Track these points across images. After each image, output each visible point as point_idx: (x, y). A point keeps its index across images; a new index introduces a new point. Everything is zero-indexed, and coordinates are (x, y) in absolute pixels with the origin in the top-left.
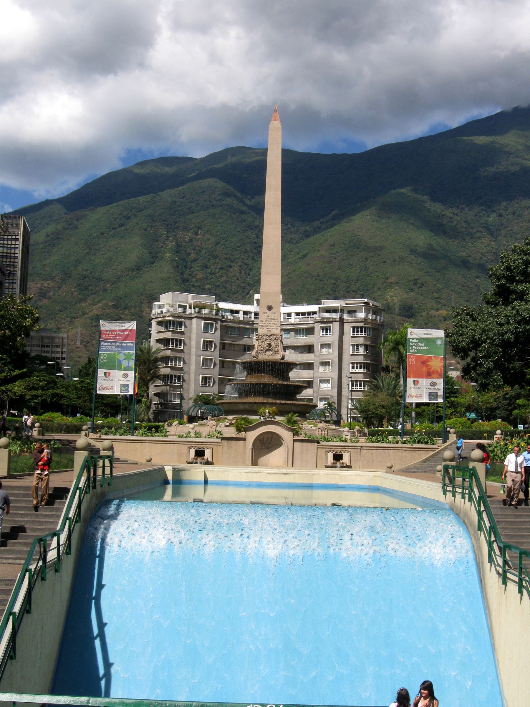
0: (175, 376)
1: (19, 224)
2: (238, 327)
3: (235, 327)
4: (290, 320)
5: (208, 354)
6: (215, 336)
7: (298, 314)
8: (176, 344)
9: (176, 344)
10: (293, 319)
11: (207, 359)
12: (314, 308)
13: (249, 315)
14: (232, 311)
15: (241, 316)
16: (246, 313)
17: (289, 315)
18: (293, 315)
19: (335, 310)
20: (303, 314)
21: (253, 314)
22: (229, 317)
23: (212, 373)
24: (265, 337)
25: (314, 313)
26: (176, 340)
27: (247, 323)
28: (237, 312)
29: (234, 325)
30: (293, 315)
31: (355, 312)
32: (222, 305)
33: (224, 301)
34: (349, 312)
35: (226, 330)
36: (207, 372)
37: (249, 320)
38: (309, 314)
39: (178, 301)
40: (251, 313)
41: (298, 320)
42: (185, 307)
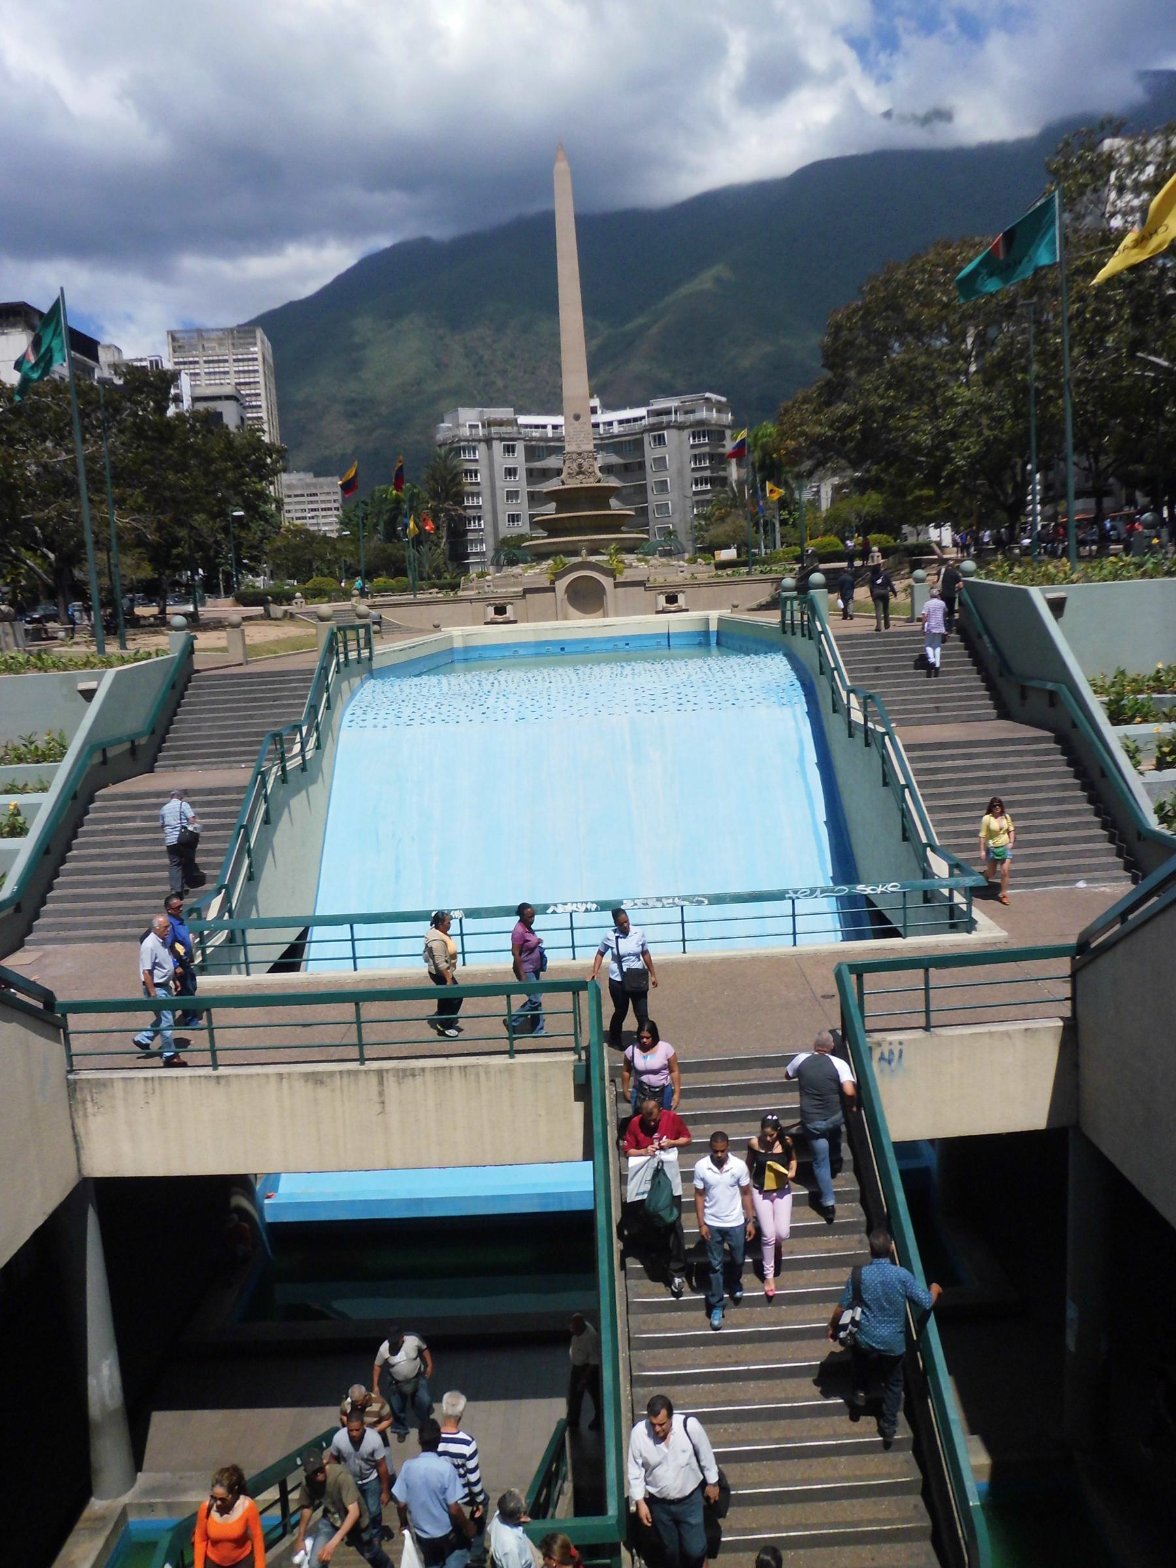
2: (547, 447)
5: (511, 484)
6: (518, 460)
7: (621, 422)
10: (616, 429)
12: (641, 412)
14: (537, 427)
16: (555, 427)
17: (610, 424)
18: (615, 424)
19: (667, 412)
20: (628, 421)
24: (574, 456)
26: (471, 471)
28: (544, 427)
29: (542, 444)
30: (615, 424)
31: (693, 412)
32: (523, 420)
33: (528, 412)
34: (687, 413)
35: (532, 453)
38: (635, 420)
42: (477, 426)
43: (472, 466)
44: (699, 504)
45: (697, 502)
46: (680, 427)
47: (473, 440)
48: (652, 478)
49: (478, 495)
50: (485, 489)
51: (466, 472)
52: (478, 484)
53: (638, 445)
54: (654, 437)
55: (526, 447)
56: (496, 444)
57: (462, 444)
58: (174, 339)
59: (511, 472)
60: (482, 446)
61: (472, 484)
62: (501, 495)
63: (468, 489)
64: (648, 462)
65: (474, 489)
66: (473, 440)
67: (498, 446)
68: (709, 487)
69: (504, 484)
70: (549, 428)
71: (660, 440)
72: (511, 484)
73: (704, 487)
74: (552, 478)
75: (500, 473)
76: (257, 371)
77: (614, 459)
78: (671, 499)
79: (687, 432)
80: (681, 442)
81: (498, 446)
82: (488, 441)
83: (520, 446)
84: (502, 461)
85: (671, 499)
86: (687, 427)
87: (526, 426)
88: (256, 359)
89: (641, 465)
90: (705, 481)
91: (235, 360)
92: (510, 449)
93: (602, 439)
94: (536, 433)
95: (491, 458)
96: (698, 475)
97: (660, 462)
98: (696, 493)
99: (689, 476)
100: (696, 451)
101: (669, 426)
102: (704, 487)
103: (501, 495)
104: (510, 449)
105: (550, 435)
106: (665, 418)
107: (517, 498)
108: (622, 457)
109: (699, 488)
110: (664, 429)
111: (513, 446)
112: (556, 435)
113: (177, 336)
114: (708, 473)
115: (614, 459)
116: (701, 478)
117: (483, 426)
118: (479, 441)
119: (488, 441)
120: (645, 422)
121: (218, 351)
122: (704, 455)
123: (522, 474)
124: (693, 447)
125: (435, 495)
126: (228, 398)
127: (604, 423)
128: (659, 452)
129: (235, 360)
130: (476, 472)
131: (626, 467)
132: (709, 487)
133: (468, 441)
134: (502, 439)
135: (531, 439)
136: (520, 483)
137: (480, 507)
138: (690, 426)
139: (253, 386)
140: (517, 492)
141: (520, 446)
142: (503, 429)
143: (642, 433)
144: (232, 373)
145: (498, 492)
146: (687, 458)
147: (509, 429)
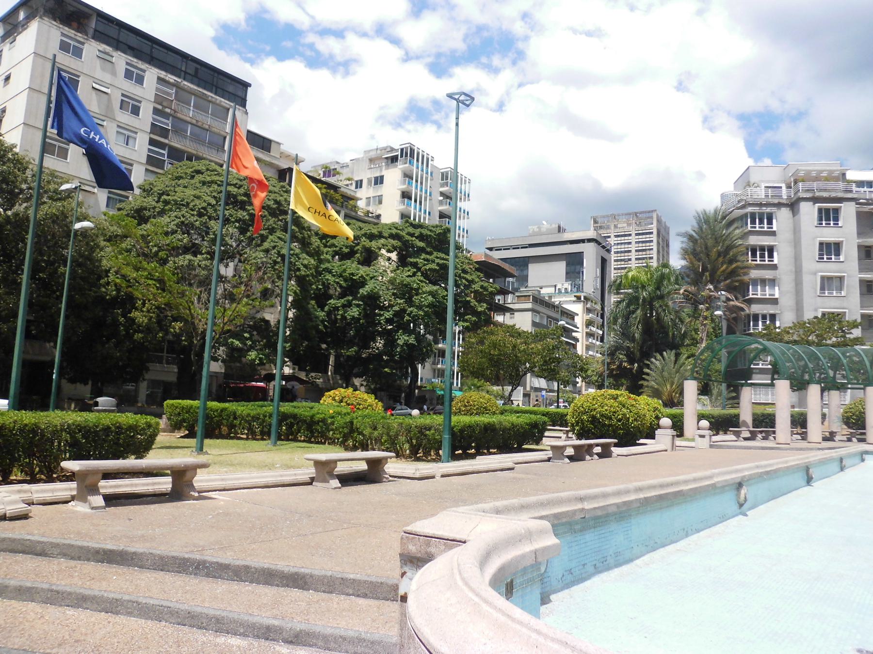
1: (652, 217)
5: (830, 269)
11: (830, 278)
23: (845, 305)
26: (762, 249)
39: (763, 181)
43: (766, 241)
47: (768, 205)
49: (773, 282)
52: (775, 267)
55: (859, 215)
57: (750, 209)
58: (595, 222)
59: (830, 249)
62: (811, 284)
63: (754, 274)
65: (767, 274)
66: (768, 205)
67: (809, 212)
69: (815, 269)
72: (830, 269)
75: (810, 250)
82: (793, 205)
83: (848, 212)
87: (861, 184)
88: (651, 233)
91: (636, 235)
92: (829, 216)
95: (796, 231)
104: (829, 216)
107: (840, 289)
111: (836, 211)
113: (599, 220)
118: (779, 205)
119: (793, 205)
121: (626, 229)
126: (590, 240)
129: (636, 235)
130: (771, 250)
133: (761, 205)
134: (815, 200)
137: (774, 301)
139: (648, 252)
140: (841, 279)
141: (848, 212)
145: (807, 279)
147: (831, 185)
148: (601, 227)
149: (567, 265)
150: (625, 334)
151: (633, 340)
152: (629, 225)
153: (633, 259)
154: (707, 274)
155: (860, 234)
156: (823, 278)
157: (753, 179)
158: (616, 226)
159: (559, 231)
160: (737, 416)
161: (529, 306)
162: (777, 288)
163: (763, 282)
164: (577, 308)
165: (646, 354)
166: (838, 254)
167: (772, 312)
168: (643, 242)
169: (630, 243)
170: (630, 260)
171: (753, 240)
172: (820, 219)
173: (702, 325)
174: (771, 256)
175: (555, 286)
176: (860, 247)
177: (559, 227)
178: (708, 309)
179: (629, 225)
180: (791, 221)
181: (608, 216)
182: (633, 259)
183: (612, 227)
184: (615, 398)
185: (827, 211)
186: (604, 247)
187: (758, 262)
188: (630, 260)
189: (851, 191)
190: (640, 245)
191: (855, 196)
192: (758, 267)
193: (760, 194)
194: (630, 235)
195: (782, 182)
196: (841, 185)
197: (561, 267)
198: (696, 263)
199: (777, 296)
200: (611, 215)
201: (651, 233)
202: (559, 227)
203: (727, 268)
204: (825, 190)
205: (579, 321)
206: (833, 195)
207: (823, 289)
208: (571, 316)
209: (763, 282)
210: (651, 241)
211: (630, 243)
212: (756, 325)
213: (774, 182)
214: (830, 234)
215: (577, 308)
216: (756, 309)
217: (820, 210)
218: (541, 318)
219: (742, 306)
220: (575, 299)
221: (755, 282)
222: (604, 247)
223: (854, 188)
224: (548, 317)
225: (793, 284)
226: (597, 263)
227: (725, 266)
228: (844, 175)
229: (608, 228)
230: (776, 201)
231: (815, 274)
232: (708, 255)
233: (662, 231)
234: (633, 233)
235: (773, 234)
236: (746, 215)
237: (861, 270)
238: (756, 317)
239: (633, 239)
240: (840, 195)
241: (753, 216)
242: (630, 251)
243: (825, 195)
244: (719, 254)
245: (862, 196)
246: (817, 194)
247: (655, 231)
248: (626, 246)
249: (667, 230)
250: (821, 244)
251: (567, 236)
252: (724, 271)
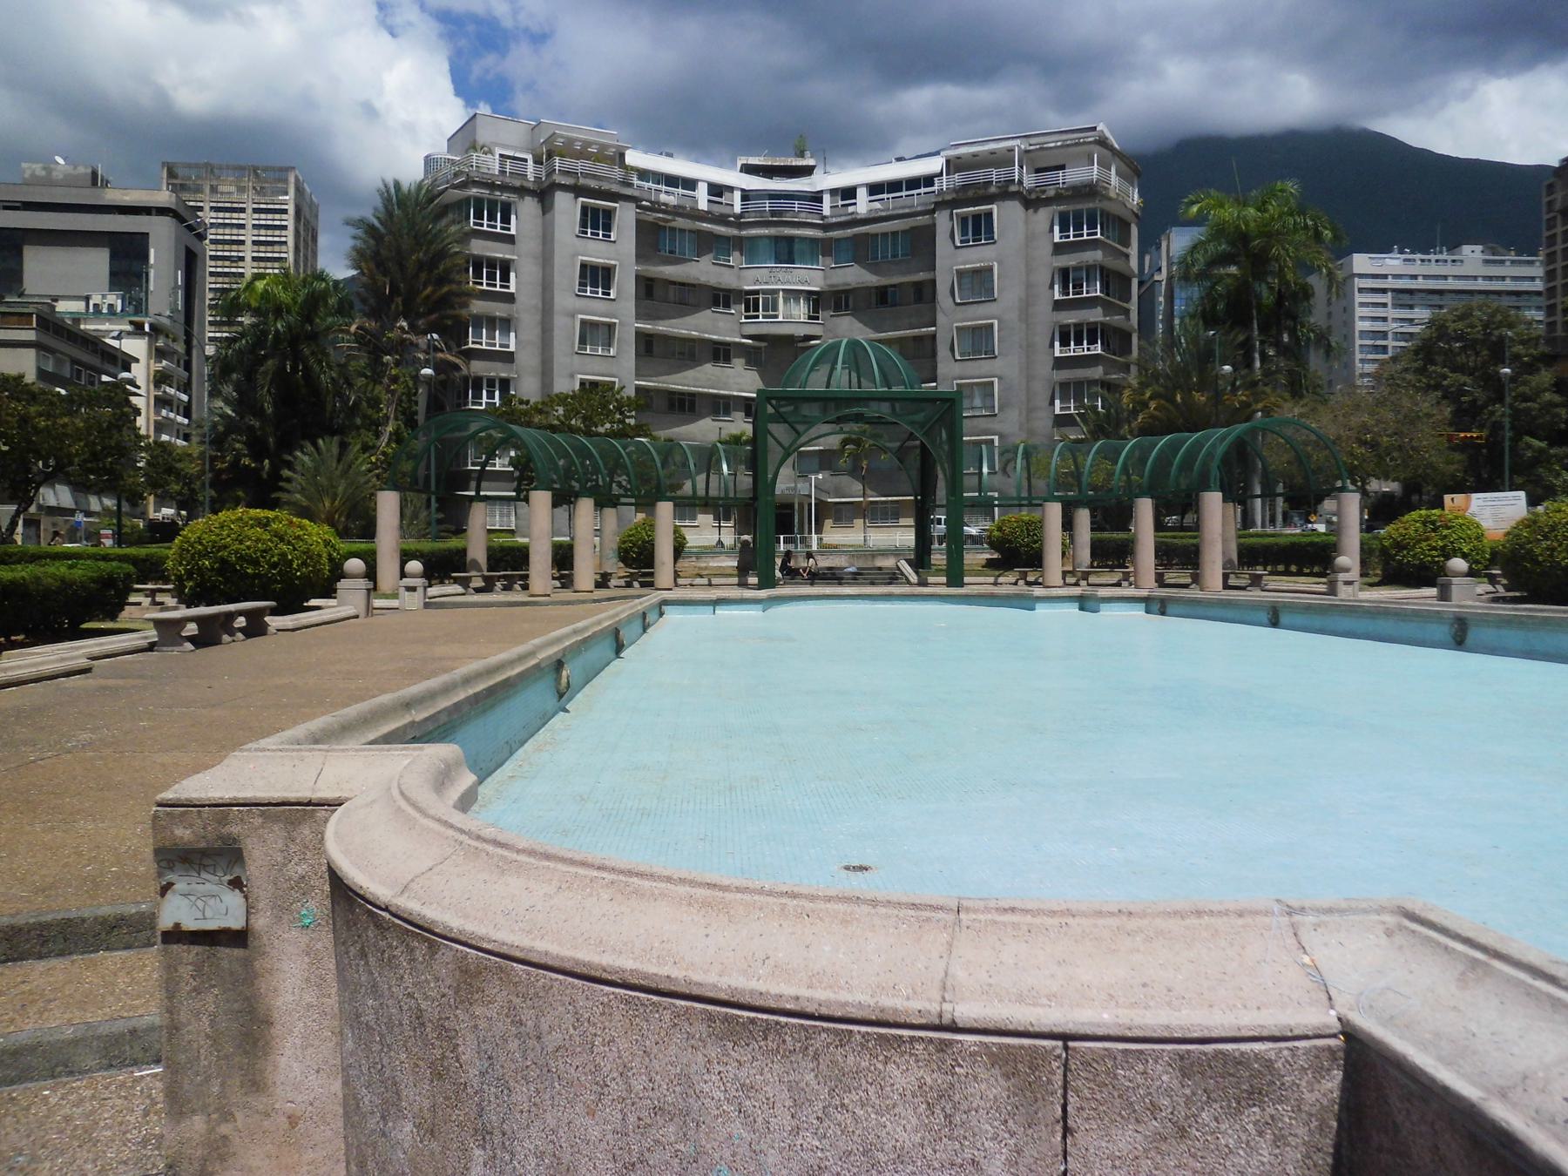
0: (491, 383)
1: (286, 181)
3: (682, 231)
4: (851, 209)
5: (595, 309)
6: (619, 248)
7: (875, 189)
8: (491, 277)
9: (491, 277)
10: (862, 205)
13: (727, 194)
14: (672, 181)
15: (702, 199)
16: (717, 190)
17: (849, 193)
18: (862, 194)
20: (894, 186)
21: (737, 195)
22: (663, 198)
23: (614, 371)
25: (928, 180)
26: (492, 263)
27: (722, 220)
28: (690, 184)
29: (680, 223)
30: (862, 194)
35: (655, 236)
36: (597, 365)
37: (726, 210)
38: (913, 183)
40: (731, 189)
41: (877, 205)
43: (498, 251)
44: (1066, 390)
45: (1064, 386)
46: (1031, 202)
47: (504, 188)
48: (950, 318)
49: (506, 324)
50: (526, 310)
51: (478, 263)
52: (510, 298)
53: (920, 242)
54: (964, 220)
55: (640, 224)
56: (562, 200)
57: (474, 191)
58: (172, 174)
59: (597, 276)
60: (527, 208)
61: (486, 296)
62: (566, 332)
63: (478, 307)
64: (944, 280)
66: (504, 188)
67: (567, 208)
68: (1098, 349)
70: (702, 190)
71: (979, 229)
72: (595, 309)
73: (1084, 350)
74: (696, 308)
76: (284, 228)
77: (854, 275)
78: (1002, 369)
79: (1043, 215)
80: (1030, 238)
81: (567, 208)
82: (544, 194)
83: (626, 217)
84: (575, 249)
85: (1002, 369)
86: (1048, 202)
87: (644, 174)
88: (285, 211)
89: (924, 294)
90: (1092, 333)
91: (256, 211)
92: (596, 221)
93: (826, 227)
94: (670, 197)
95: (547, 239)
96: (1070, 318)
97: (978, 282)
98: (1060, 363)
99: (1046, 319)
100: (1069, 260)
101: (1005, 193)
102: (1084, 350)
103: (566, 332)
105: (703, 205)
106: (995, 175)
107: (608, 344)
108: (874, 268)
109: (1073, 350)
110: (991, 199)
111: (609, 214)
112: (717, 209)
113: (180, 172)
114: (1095, 315)
115: (854, 275)
116: (1078, 326)
117: (538, 161)
118: (522, 191)
119: (544, 194)
120: (943, 184)
121: (235, 197)
122: (1090, 269)
123: (625, 285)
124: (1059, 249)
125: (380, 309)
126: (162, 211)
127: (833, 192)
128: (974, 257)
129: (256, 211)
130: (506, 268)
131: (882, 296)
132: (1098, 349)
133: (492, 186)
134: (578, 191)
135: (656, 206)
136: (620, 306)
137: (508, 358)
138: (1058, 198)
139: (277, 248)
140: (611, 326)
141: (626, 217)
142: (580, 165)
143: (933, 211)
144: (249, 227)
145: (560, 321)
146: (1043, 276)
147: (602, 169)
148: (183, 187)
149: (112, 257)
150: (245, 403)
151: (259, 413)
152: (241, 190)
153: (248, 259)
154: (399, 300)
155: (640, 257)
156: (583, 322)
157: (483, 136)
158: (214, 190)
159: (94, 183)
160: (464, 552)
161: (30, 335)
162: (512, 335)
163: (492, 323)
164: (135, 347)
165: (288, 443)
166: (607, 286)
167: (503, 375)
168: (267, 227)
169: (242, 226)
170: (242, 259)
171: (478, 247)
172: (584, 224)
173: (388, 391)
174: (505, 278)
175: (87, 299)
176: (638, 278)
177: (94, 174)
178: (397, 364)
179: (241, 190)
180: (539, 221)
181: (197, 166)
182: (248, 259)
183: (207, 190)
184: (265, 524)
185: (595, 210)
186: (190, 228)
187: (485, 287)
188: (242, 259)
189: (630, 185)
190: (263, 232)
191: (636, 193)
192: (486, 296)
193: (492, 165)
194: (243, 210)
195: (527, 151)
196: (617, 173)
197: (98, 261)
198: (380, 277)
199: (512, 348)
200: (207, 165)
201: (285, 211)
202: (94, 174)
203: (433, 292)
204: (594, 177)
205: (140, 373)
206: (605, 186)
207: (583, 341)
208: (127, 362)
209: (492, 323)
210: (284, 228)
211: (242, 226)
212: (478, 396)
213: (515, 148)
214: (596, 252)
215: (135, 347)
216: (478, 367)
217: (584, 208)
218: (58, 362)
219: (457, 361)
220: (129, 328)
221: (479, 321)
222: (190, 228)
223: (636, 181)
224: (74, 361)
225: (538, 331)
226: (177, 257)
227: (429, 290)
228: (622, 156)
229: (198, 190)
230: (517, 183)
231: (573, 316)
232: (402, 267)
233: (306, 211)
234: (250, 207)
235: (511, 240)
236: (468, 199)
237: (638, 317)
238: (477, 384)
239: (248, 219)
240: (615, 188)
241: (479, 202)
242: (242, 242)
243: (593, 184)
244: (421, 266)
245: (645, 196)
246: (582, 181)
247: (291, 208)
248: (235, 231)
249: (314, 208)
250: (584, 266)
251: (112, 196)
252: (428, 297)
